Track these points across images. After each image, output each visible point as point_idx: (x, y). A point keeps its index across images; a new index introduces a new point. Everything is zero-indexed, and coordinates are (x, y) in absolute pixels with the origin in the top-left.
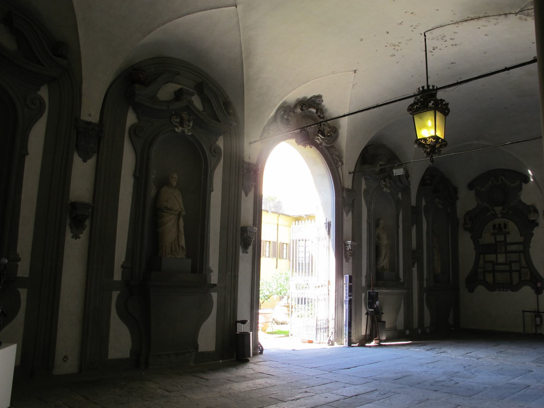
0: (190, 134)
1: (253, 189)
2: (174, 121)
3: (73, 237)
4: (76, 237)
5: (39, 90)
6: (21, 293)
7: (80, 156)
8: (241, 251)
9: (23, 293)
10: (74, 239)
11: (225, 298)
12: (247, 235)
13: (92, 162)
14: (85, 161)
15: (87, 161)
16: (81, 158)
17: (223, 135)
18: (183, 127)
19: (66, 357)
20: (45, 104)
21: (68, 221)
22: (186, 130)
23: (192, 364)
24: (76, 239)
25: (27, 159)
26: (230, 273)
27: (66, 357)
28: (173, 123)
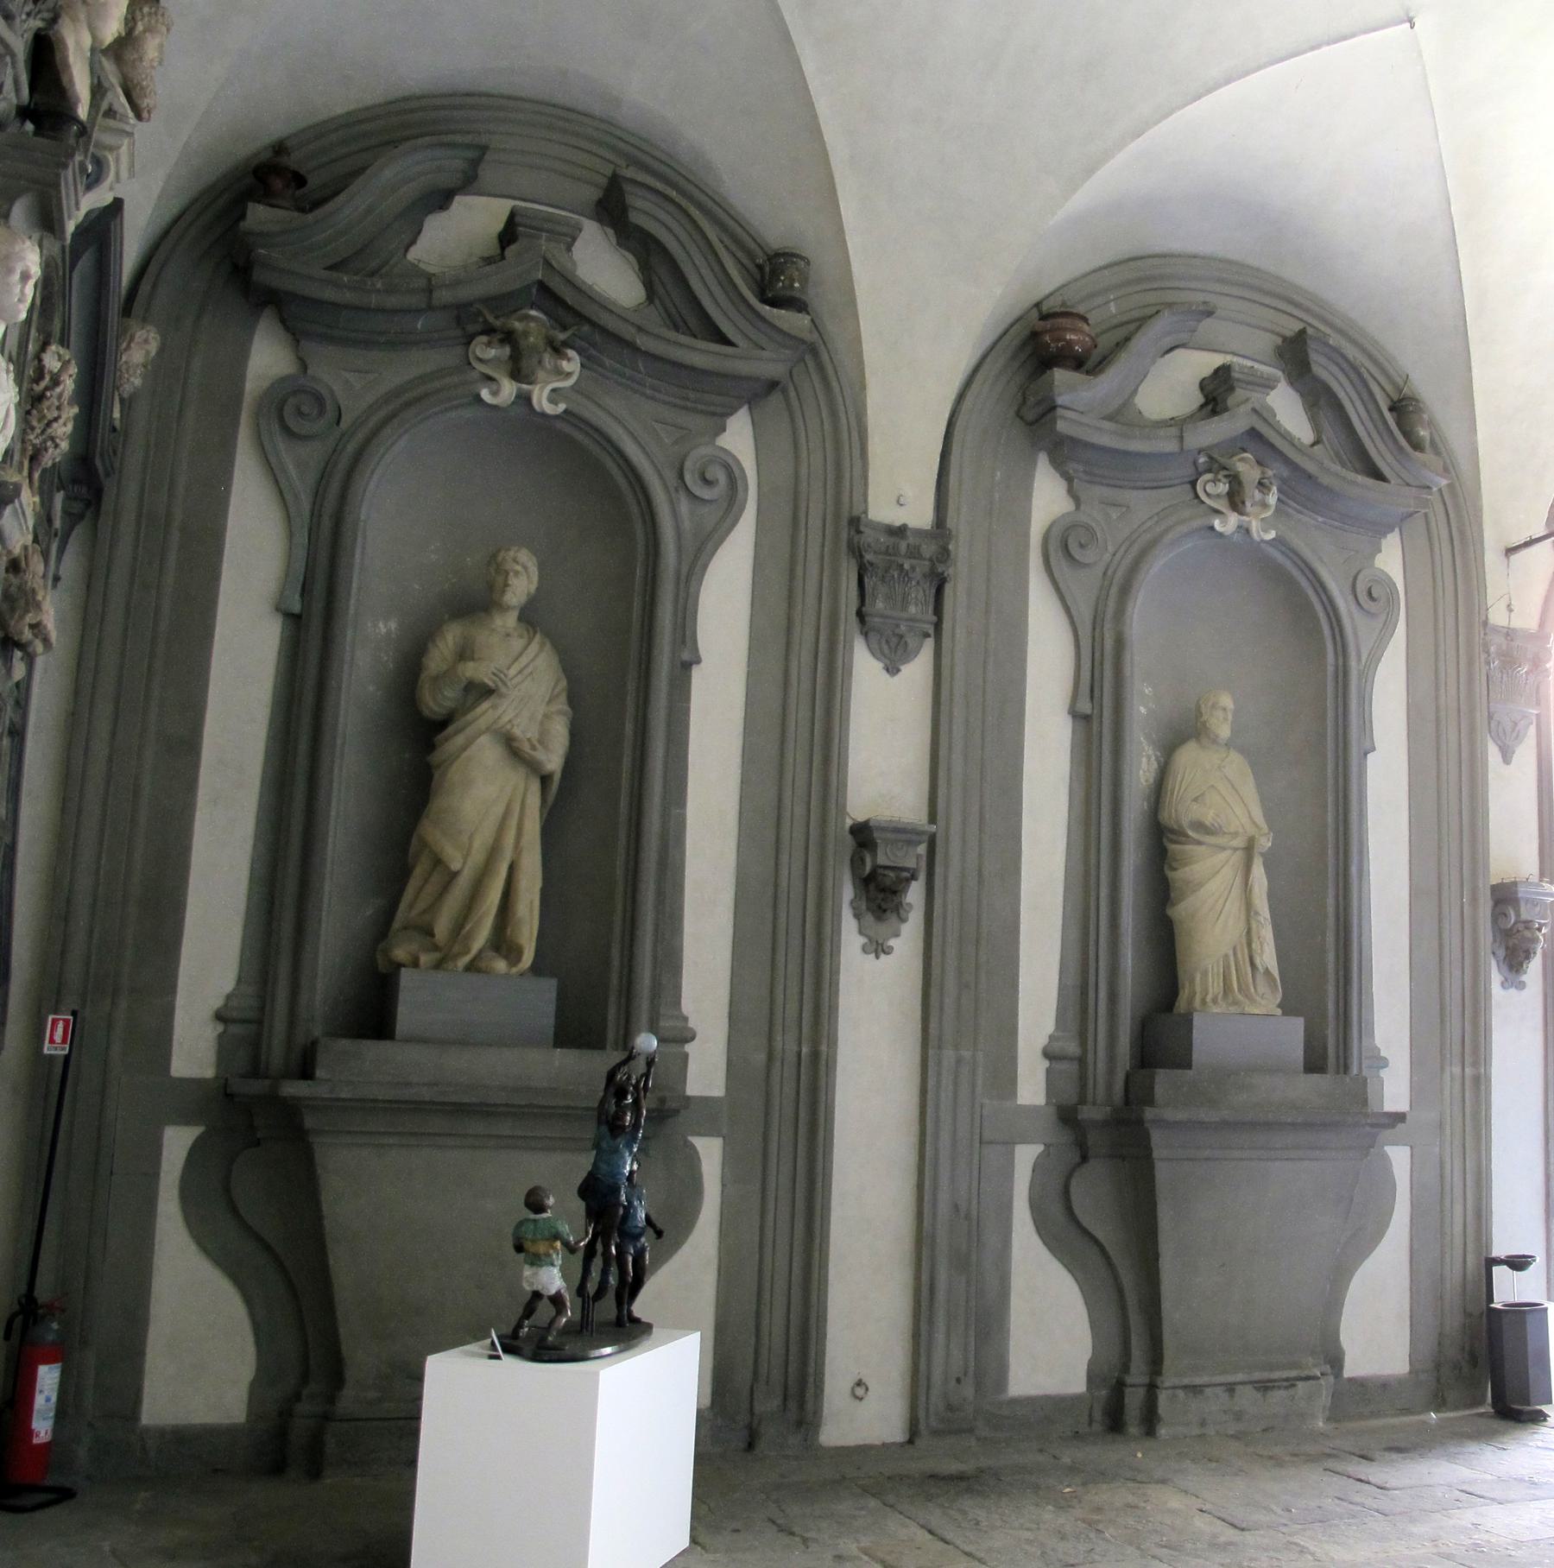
0: (1271, 535)
1: (1532, 730)
2: (1208, 495)
4: (878, 948)
8: (1496, 978)
9: (710, 1152)
11: (1442, 1167)
12: (1518, 914)
13: (918, 669)
14: (892, 670)
15: (898, 670)
17: (1397, 530)
18: (1241, 513)
19: (859, 1383)
21: (848, 892)
22: (1255, 526)
23: (1321, 1424)
24: (877, 957)
25: (697, 674)
26: (1457, 1070)
27: (859, 1383)
28: (1203, 502)
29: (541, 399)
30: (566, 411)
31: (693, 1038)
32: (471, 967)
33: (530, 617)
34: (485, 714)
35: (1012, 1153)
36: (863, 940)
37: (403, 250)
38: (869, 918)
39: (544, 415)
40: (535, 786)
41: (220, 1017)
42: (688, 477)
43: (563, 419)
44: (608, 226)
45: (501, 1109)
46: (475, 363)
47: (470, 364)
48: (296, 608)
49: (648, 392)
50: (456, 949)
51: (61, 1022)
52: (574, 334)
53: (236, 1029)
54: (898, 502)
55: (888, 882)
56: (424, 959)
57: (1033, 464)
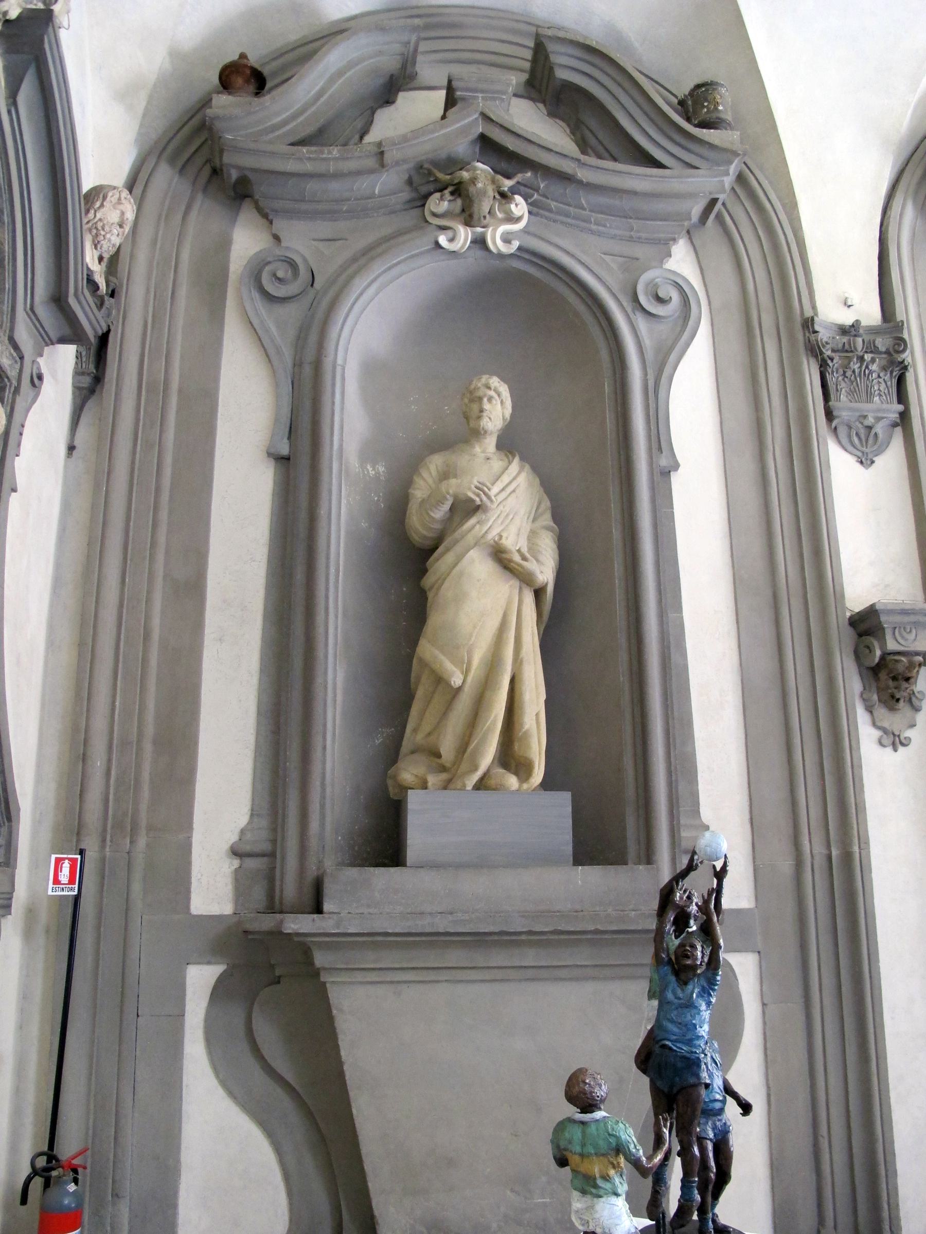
14: (866, 461)
15: (873, 462)
21: (856, 685)
24: (895, 750)
25: (677, 481)
30: (520, 248)
32: (481, 785)
36: (877, 733)
37: (357, 137)
38: (881, 712)
39: (501, 256)
40: (529, 599)
41: (235, 852)
42: (642, 299)
43: (518, 256)
44: (539, 102)
45: (523, 937)
46: (430, 219)
47: (427, 222)
48: (285, 450)
49: (594, 227)
50: (464, 767)
51: (67, 861)
52: (518, 183)
53: (251, 863)
54: (845, 304)
55: (900, 668)
56: (432, 780)
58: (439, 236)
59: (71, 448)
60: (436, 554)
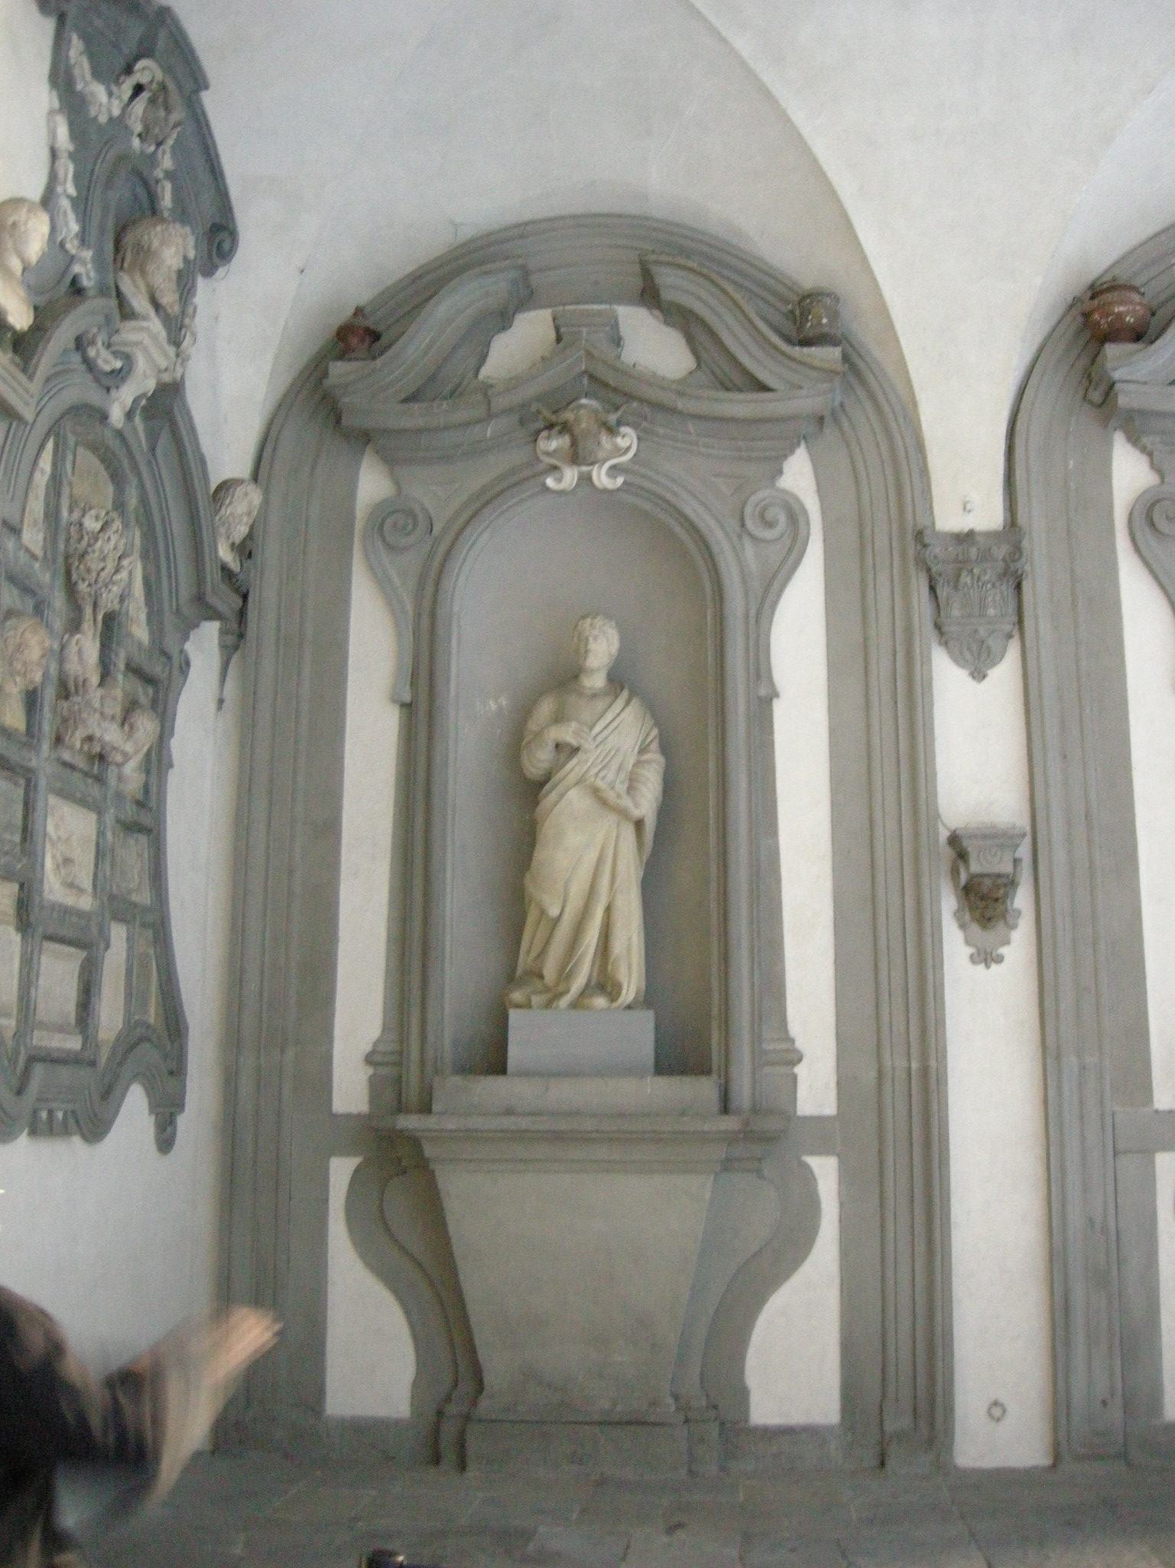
3: (973, 960)
4: (986, 957)
5: (780, 472)
6: (817, 1171)
7: (958, 659)
9: (825, 1171)
10: (982, 967)
13: (1005, 673)
14: (979, 675)
15: (984, 677)
16: (963, 667)
19: (996, 1404)
20: (805, 512)
21: (948, 903)
24: (988, 967)
25: (779, 709)
29: (601, 477)
30: (625, 483)
31: (800, 1060)
32: (575, 1005)
33: (619, 680)
34: (574, 768)
35: (1152, 1163)
36: (970, 950)
38: (975, 928)
39: (605, 491)
40: (628, 833)
41: (369, 1059)
42: (749, 523)
46: (543, 458)
48: (407, 698)
49: (703, 450)
50: (561, 988)
54: (965, 508)
55: (985, 889)
56: (536, 1000)
57: (1109, 445)
58: (545, 479)
59: (221, 702)
60: (547, 787)
